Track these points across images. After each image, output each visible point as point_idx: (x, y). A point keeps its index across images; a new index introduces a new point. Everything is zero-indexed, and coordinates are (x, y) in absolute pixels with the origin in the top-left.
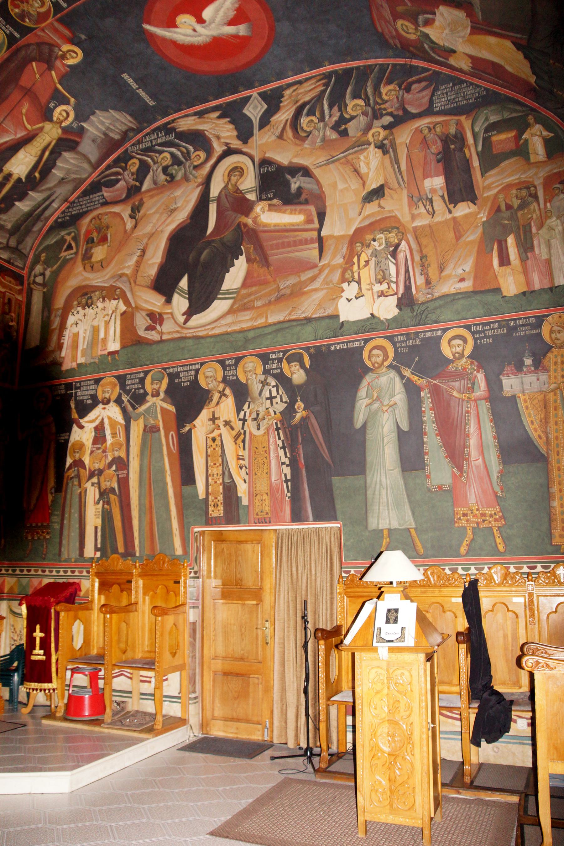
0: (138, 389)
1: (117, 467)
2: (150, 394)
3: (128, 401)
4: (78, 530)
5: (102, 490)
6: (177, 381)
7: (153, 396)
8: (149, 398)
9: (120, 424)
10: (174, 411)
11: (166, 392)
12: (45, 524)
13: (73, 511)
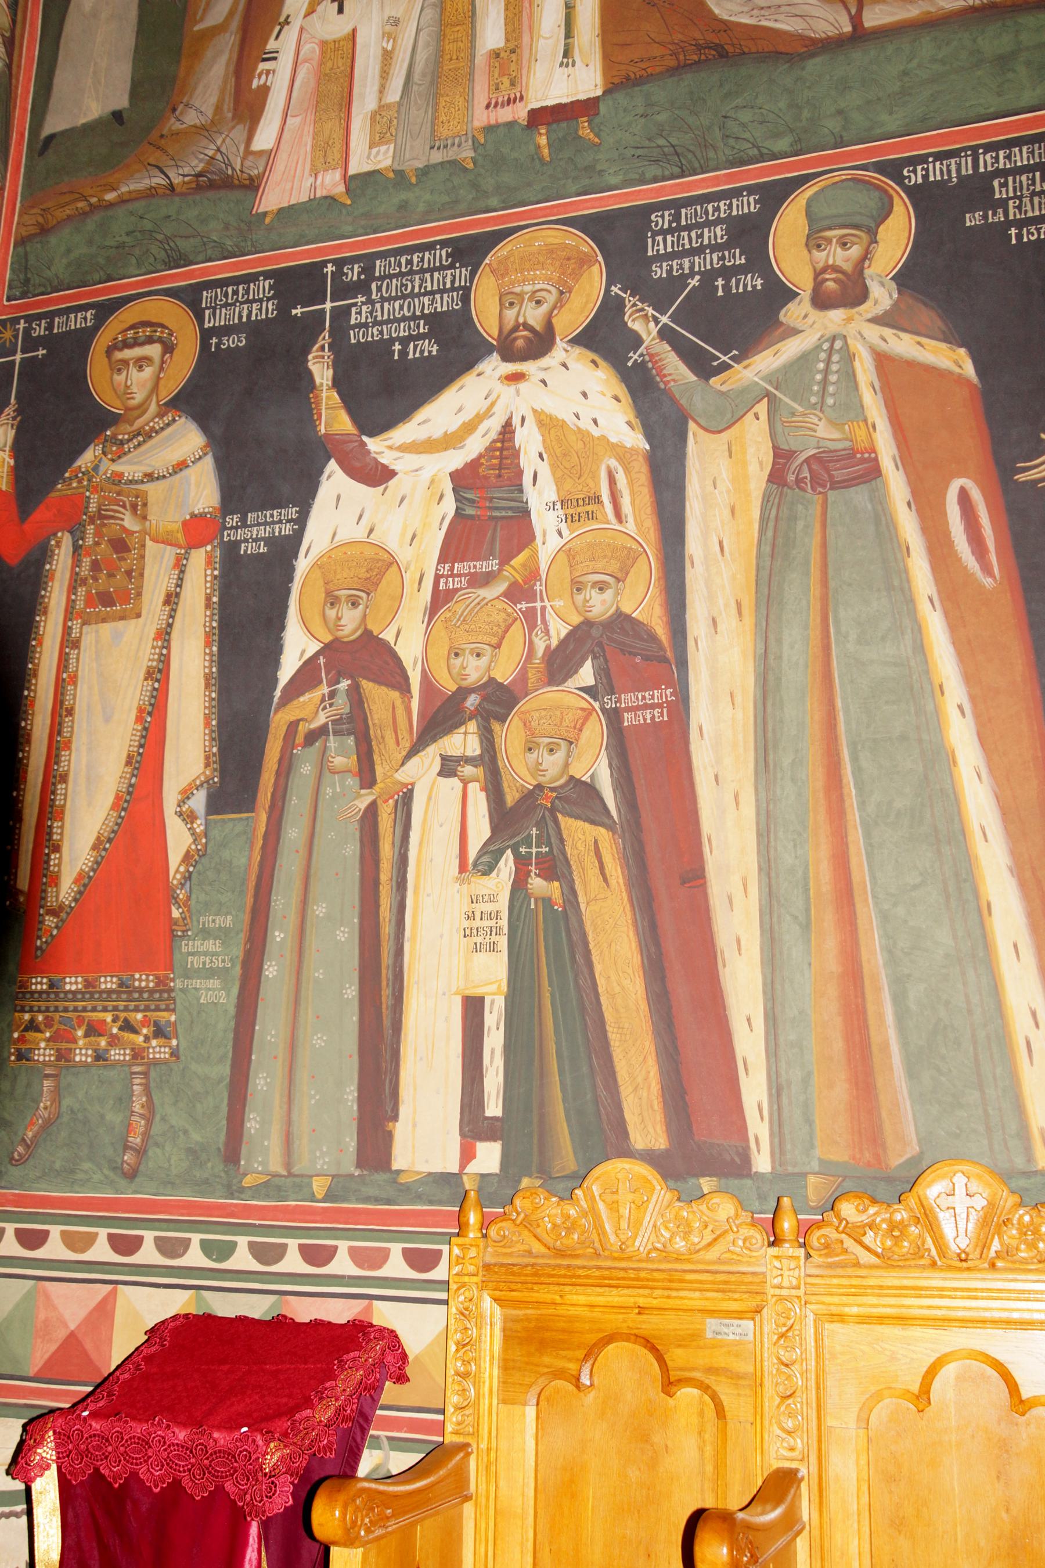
0: (727, 273)
1: (603, 672)
2: (806, 295)
3: (665, 334)
4: (353, 1019)
5: (511, 798)
6: (973, 220)
7: (822, 301)
8: (793, 313)
9: (622, 453)
10: (969, 369)
11: (904, 279)
12: (143, 980)
13: (319, 910)
